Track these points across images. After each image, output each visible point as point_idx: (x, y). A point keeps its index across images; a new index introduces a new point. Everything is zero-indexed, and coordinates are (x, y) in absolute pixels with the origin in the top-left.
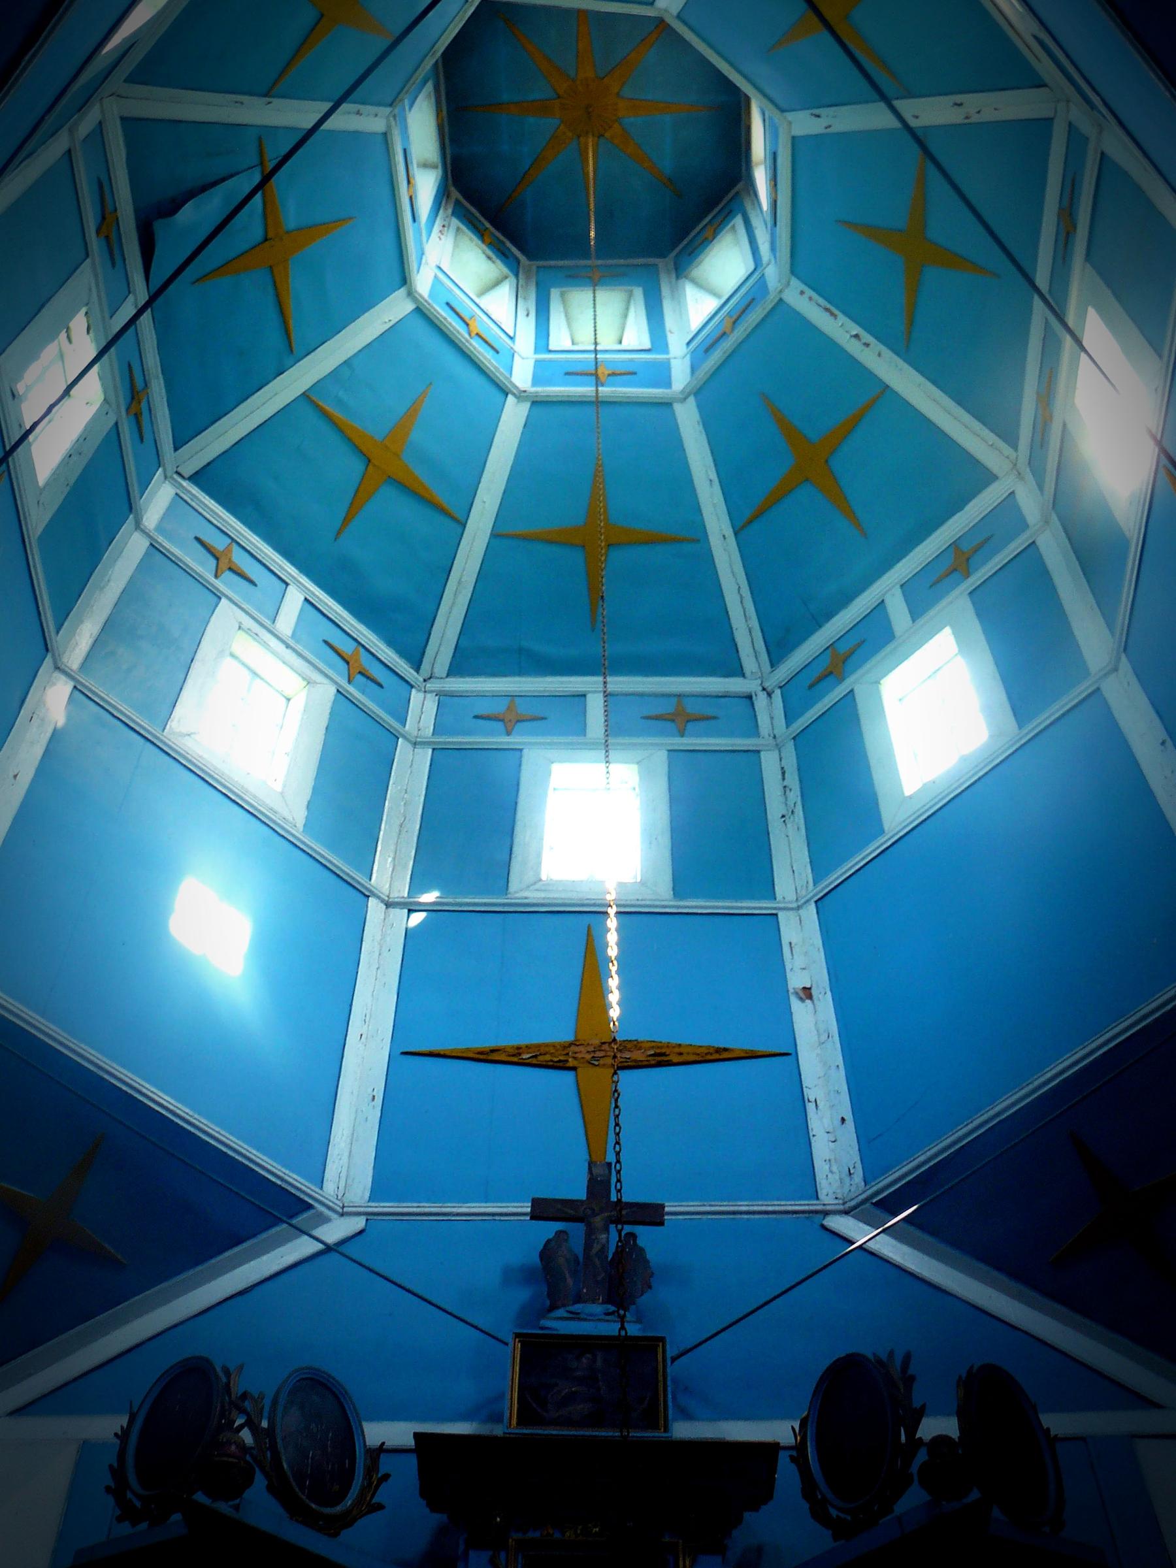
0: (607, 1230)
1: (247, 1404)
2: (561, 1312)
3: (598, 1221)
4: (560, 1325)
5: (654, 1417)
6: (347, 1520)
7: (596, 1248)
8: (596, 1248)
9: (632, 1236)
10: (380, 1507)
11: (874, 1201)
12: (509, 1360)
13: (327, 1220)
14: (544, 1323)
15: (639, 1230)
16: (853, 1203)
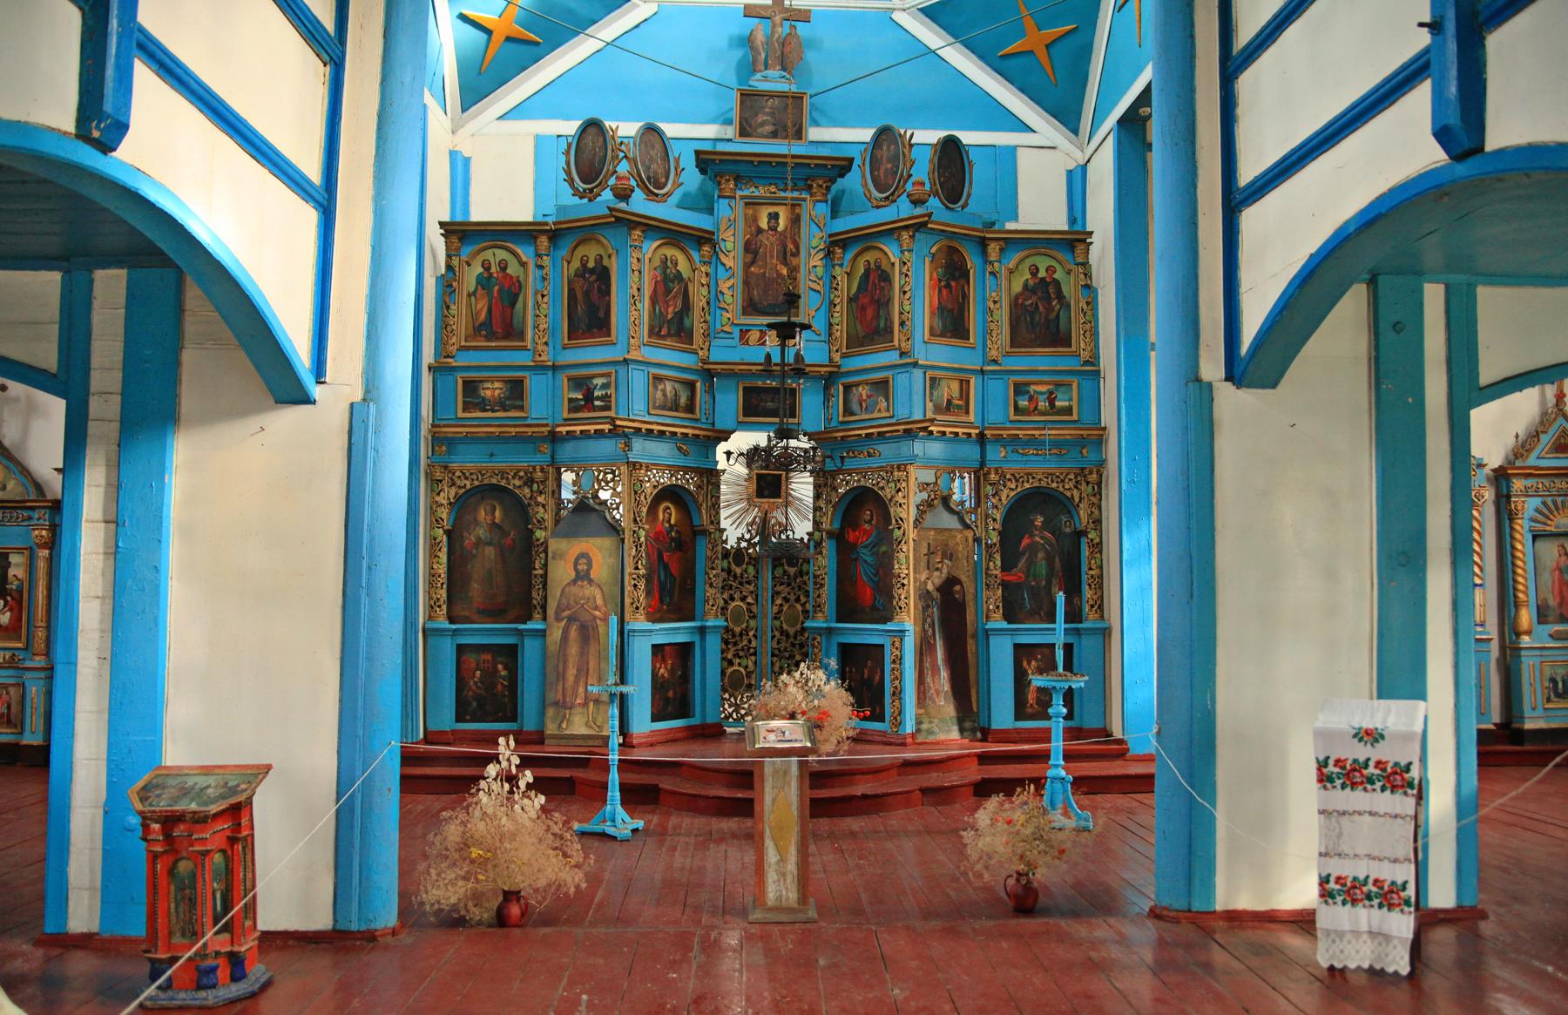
0: (782, 25)
1: (623, 147)
2: (758, 76)
3: (778, 19)
4: (758, 83)
5: (799, 134)
6: (668, 195)
7: (777, 36)
8: (777, 36)
9: (795, 27)
10: (682, 184)
11: (919, 7)
12: (736, 96)
13: (638, 6)
14: (751, 83)
15: (798, 24)
16: (908, 6)
